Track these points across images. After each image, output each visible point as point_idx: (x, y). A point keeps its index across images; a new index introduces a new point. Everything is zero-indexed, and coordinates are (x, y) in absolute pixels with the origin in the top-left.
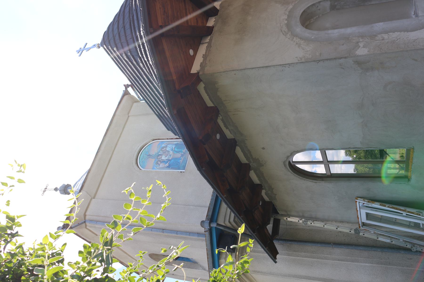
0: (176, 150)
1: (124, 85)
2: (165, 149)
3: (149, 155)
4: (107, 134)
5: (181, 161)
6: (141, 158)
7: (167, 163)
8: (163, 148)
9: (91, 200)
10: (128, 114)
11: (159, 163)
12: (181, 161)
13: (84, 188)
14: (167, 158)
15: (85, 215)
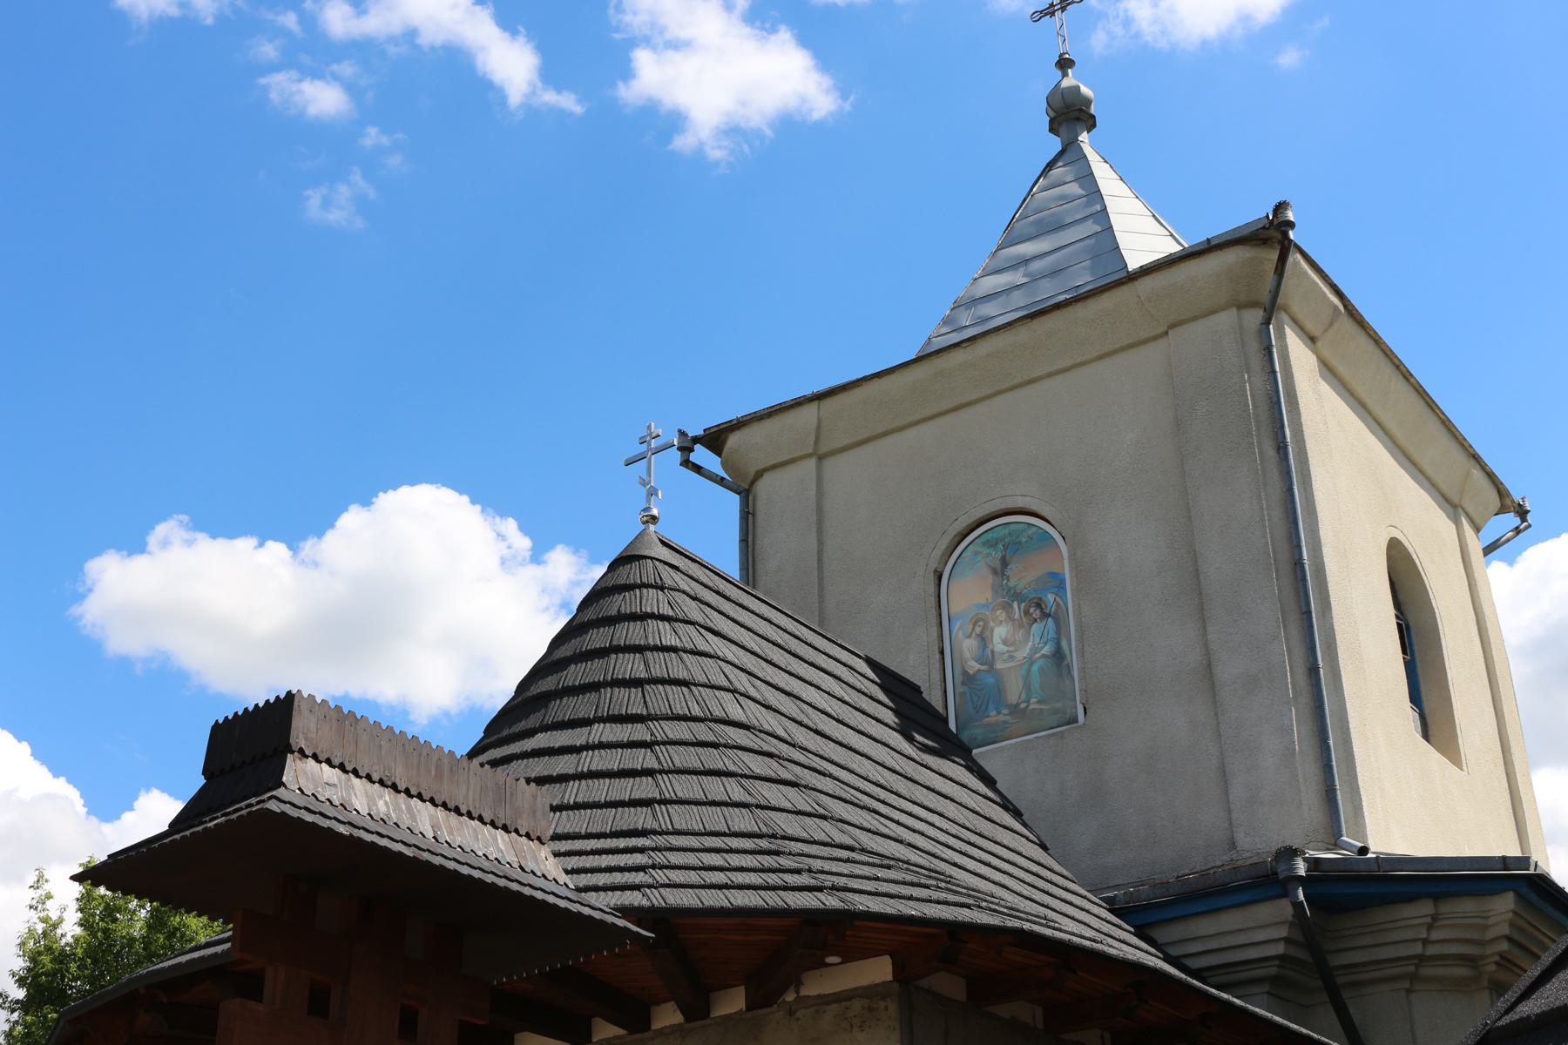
0: (1035, 668)
1: (1280, 207)
2: (1036, 613)
3: (1005, 563)
4: (1043, 319)
5: (993, 717)
6: (990, 535)
7: (980, 661)
8: (1038, 605)
9: (809, 456)
10: (1173, 326)
11: (978, 630)
12: (993, 717)
13: (828, 404)
14: (999, 647)
15: (759, 475)
